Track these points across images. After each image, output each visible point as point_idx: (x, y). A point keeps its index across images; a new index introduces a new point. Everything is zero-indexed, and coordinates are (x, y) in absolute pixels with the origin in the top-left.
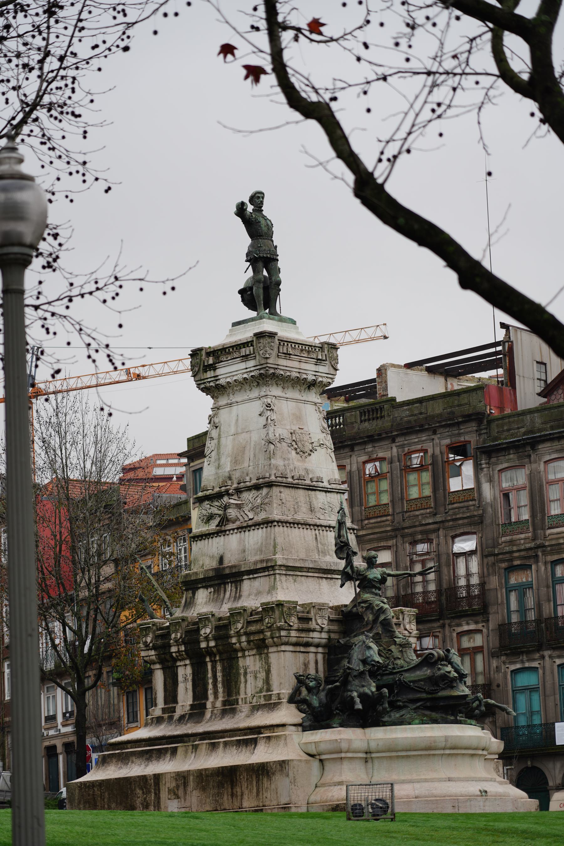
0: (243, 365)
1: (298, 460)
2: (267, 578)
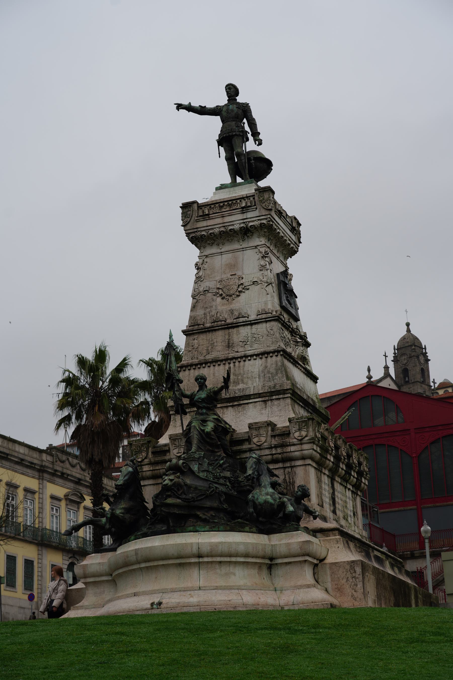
1: (223, 305)
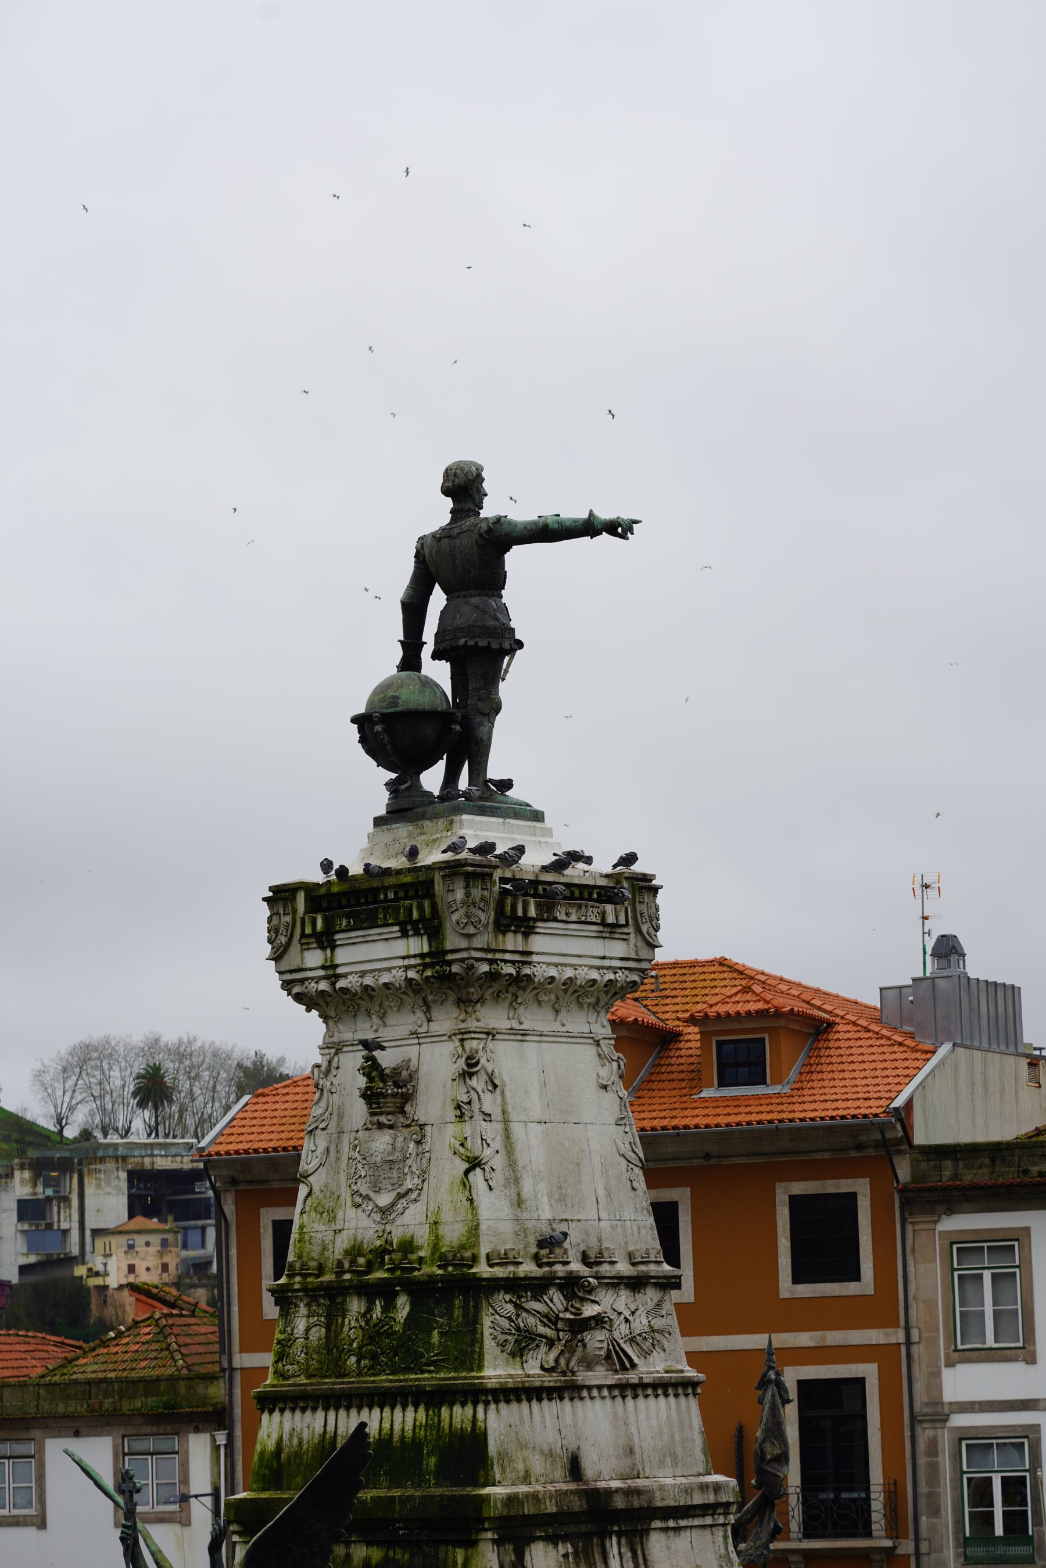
0: (597, 947)
2: (707, 1532)
